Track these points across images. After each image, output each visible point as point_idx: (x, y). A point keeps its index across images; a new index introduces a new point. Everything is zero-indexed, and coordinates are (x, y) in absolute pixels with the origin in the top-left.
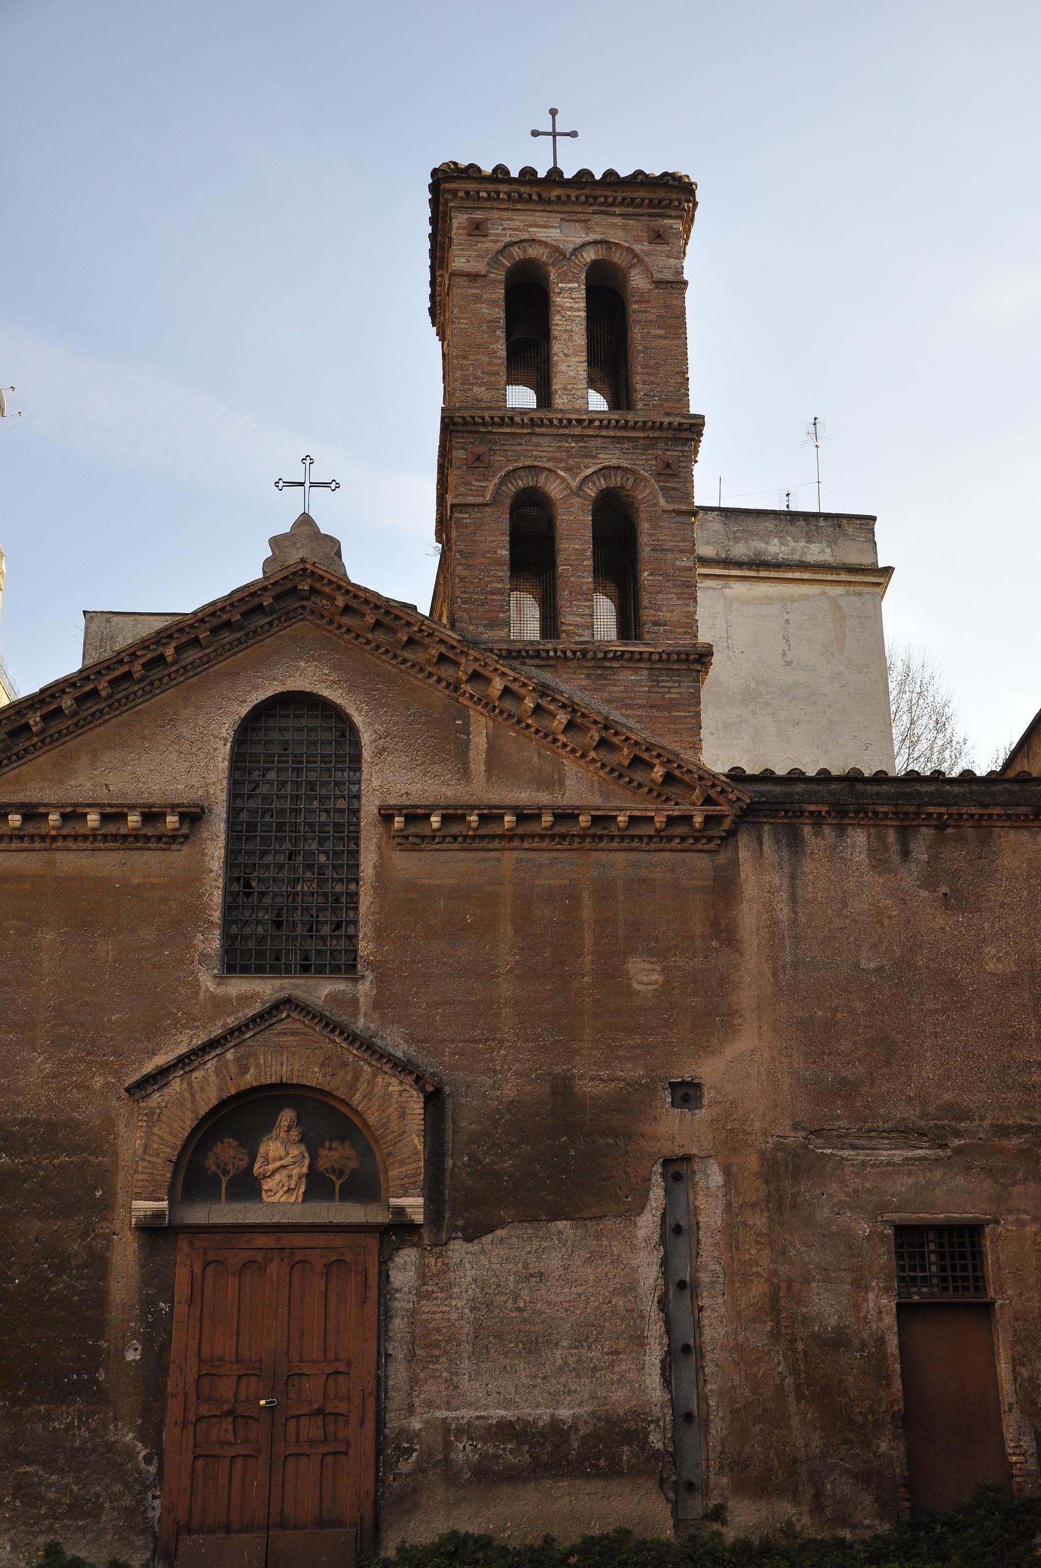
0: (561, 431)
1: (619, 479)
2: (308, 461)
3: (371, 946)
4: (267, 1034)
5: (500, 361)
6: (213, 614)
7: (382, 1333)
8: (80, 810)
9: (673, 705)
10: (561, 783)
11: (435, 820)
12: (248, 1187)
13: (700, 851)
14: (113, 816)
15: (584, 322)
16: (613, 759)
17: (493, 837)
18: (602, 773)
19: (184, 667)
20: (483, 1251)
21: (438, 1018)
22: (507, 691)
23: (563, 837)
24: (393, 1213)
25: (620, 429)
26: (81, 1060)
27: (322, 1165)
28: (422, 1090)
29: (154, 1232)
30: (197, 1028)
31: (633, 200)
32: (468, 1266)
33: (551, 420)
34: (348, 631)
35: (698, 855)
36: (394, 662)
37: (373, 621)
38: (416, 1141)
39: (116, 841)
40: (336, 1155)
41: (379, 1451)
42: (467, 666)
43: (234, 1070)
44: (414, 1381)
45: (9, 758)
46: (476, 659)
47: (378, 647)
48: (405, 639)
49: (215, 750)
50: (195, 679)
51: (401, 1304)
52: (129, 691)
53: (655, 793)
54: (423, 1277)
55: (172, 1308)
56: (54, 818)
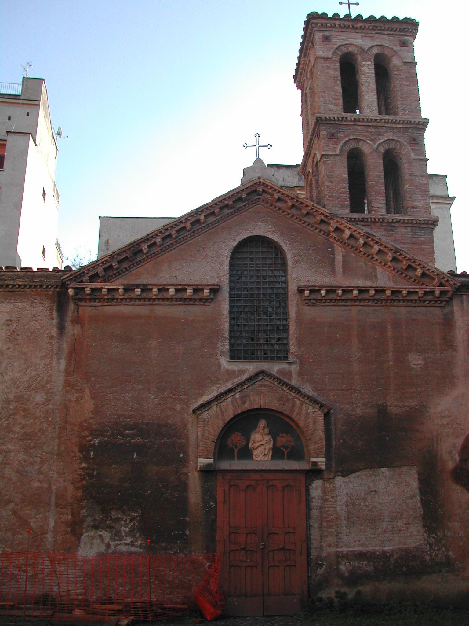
0: (368, 124)
1: (394, 145)
2: (257, 136)
3: (296, 348)
4: (253, 386)
5: (339, 94)
6: (221, 201)
7: (308, 516)
8: (166, 287)
9: (422, 243)
10: (376, 276)
11: (323, 292)
12: (246, 453)
13: (437, 307)
14: (181, 290)
15: (374, 78)
16: (399, 266)
17: (347, 300)
18: (393, 272)
19: (208, 225)
20: (350, 482)
21: (327, 380)
22: (351, 236)
23: (378, 300)
24: (312, 465)
25: (393, 123)
26: (171, 397)
27: (279, 444)
28: (323, 411)
29: (207, 473)
30: (220, 384)
31: (392, 28)
32: (344, 487)
34: (279, 209)
35: (436, 308)
36: (300, 223)
37: (291, 205)
38: (321, 434)
39: (181, 301)
40: (284, 439)
41: (309, 565)
42: (334, 225)
43: (239, 402)
44: (322, 536)
45: (133, 265)
46: (337, 222)
47: (293, 216)
48: (306, 212)
49: (223, 261)
50: (212, 230)
51: (315, 503)
52: (185, 235)
53: (417, 281)
54: (325, 492)
55: (216, 504)
56: (155, 290)
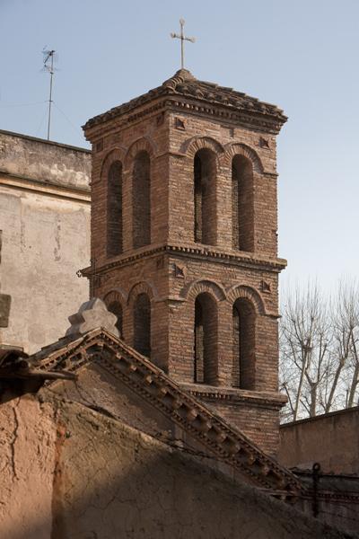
16: (242, 460)
33: (218, 254)
